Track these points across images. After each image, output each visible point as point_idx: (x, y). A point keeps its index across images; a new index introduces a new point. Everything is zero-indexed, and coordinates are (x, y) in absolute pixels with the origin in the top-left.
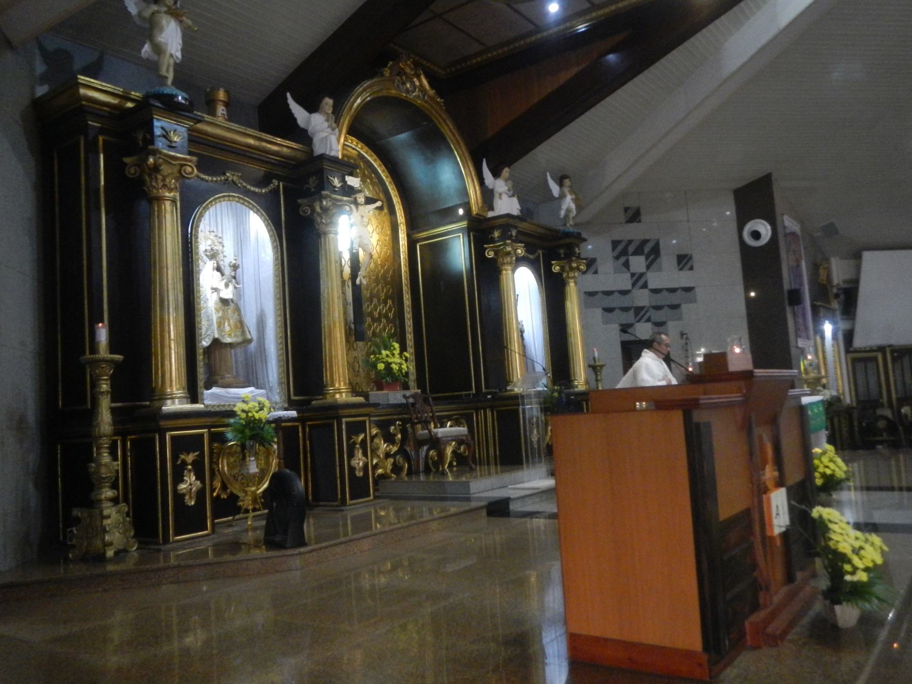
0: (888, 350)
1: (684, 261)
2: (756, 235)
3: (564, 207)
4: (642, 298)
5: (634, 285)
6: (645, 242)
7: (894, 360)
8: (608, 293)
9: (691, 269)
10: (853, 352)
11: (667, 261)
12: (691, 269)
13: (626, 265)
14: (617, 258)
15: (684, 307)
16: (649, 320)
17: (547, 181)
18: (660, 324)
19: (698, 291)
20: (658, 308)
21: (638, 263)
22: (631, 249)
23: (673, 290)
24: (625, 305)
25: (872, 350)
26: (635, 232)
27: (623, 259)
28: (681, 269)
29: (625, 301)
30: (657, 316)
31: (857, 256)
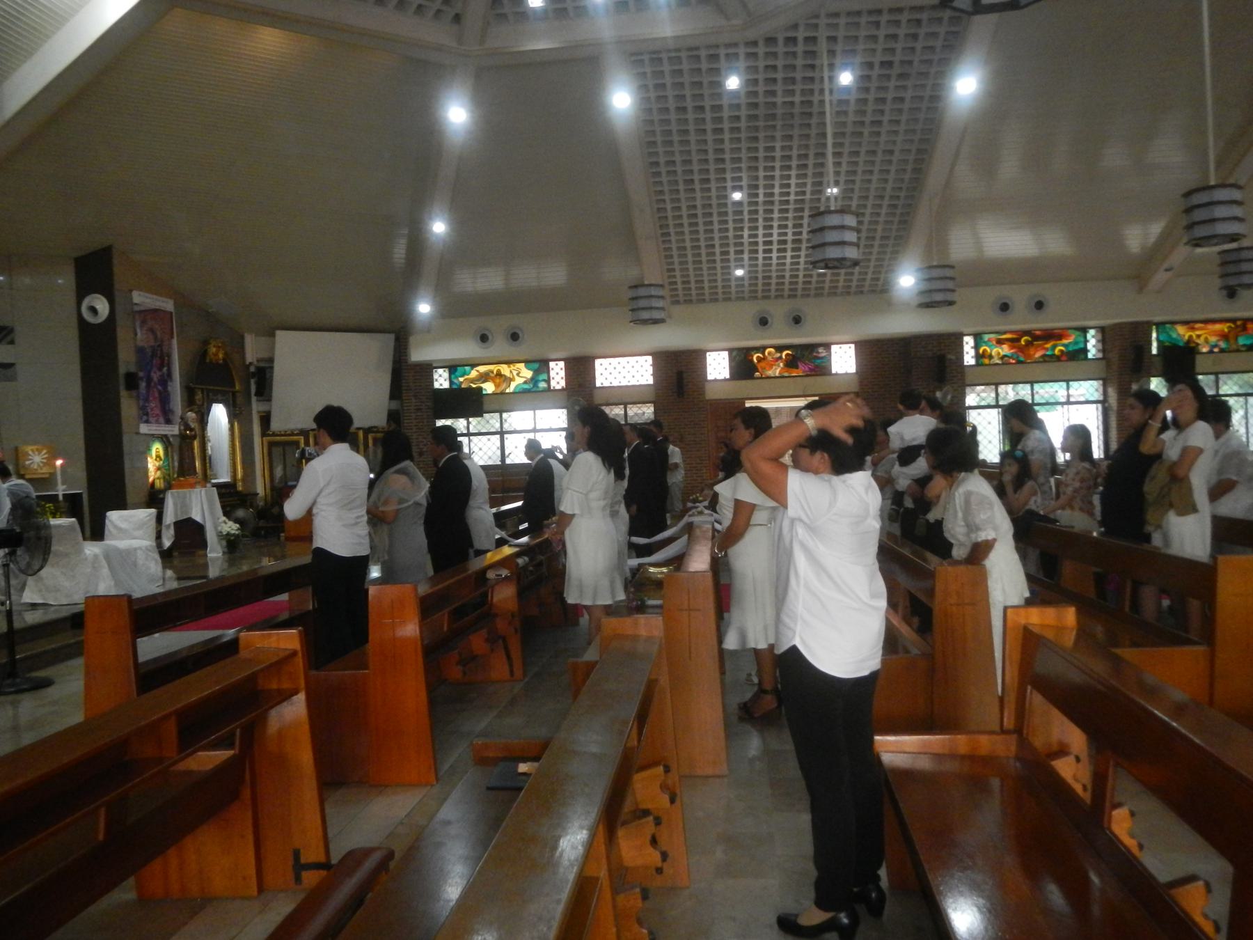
2: (93, 310)
9: (12, 342)
10: (269, 435)
25: (292, 434)
31: (272, 334)
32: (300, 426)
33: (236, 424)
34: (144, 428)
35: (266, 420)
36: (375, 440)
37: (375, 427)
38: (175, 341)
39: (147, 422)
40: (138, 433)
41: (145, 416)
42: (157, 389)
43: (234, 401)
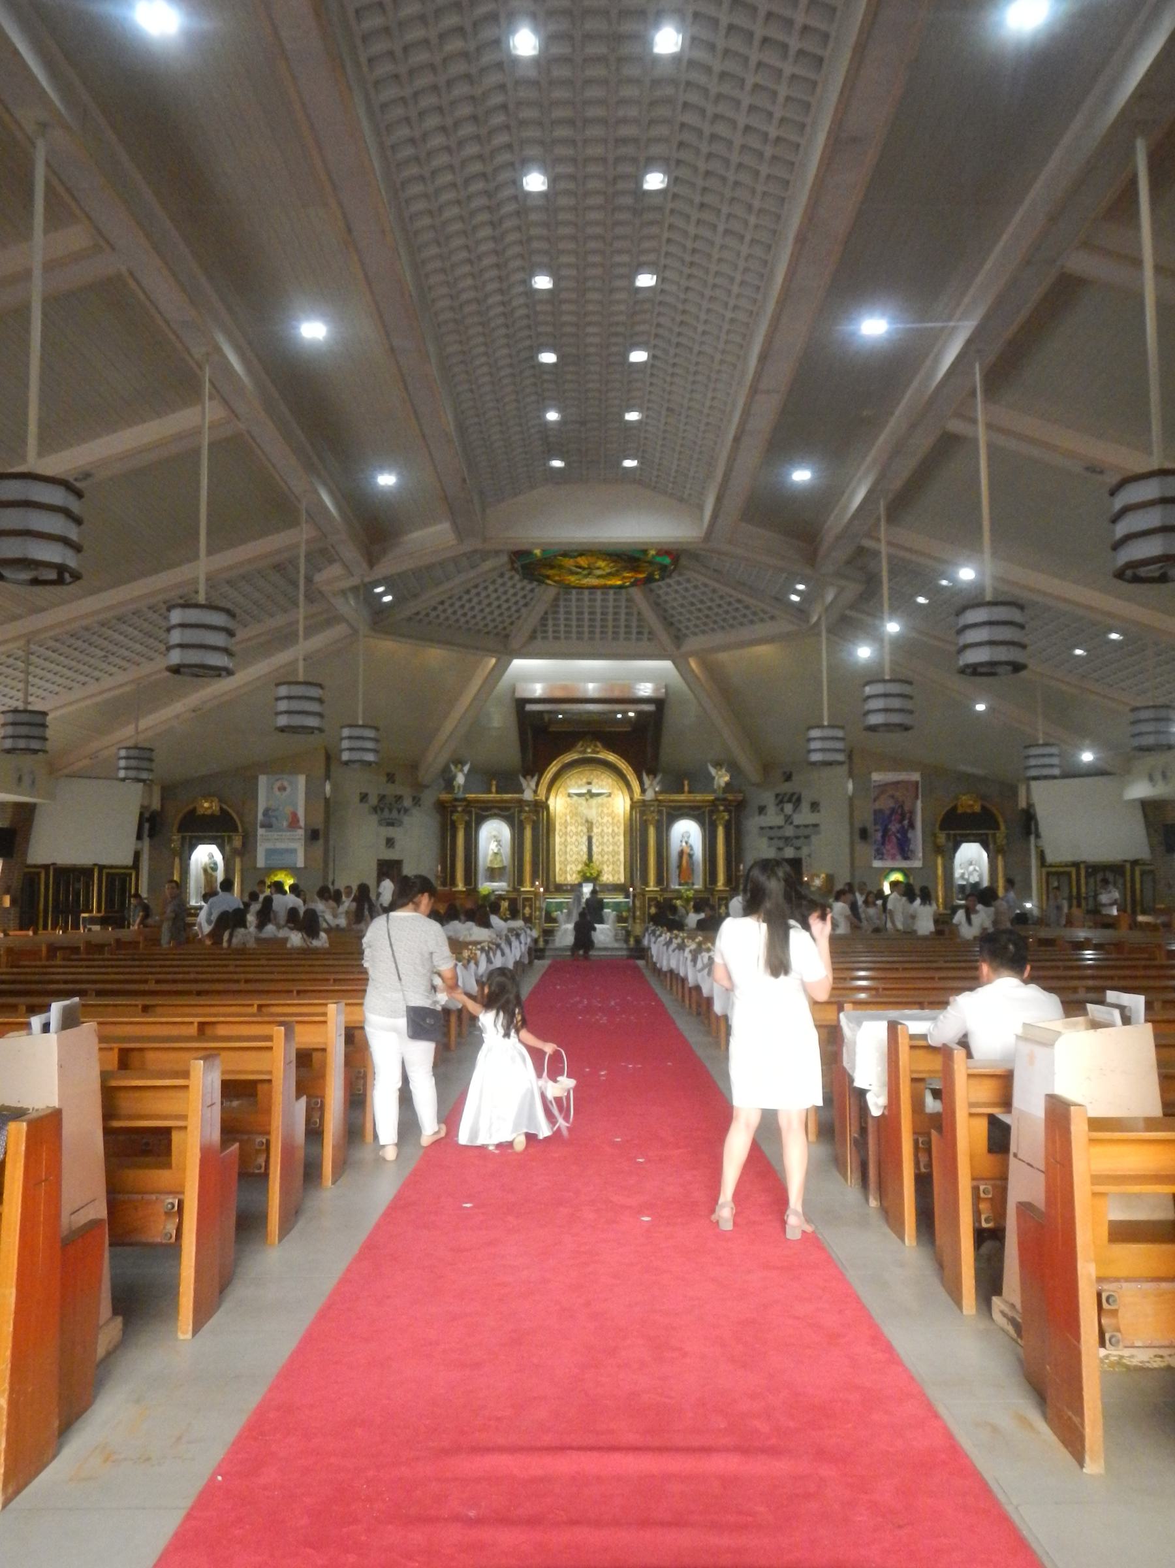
0: (1082, 866)
1: (815, 806)
3: (716, 782)
4: (789, 831)
5: (786, 821)
6: (793, 794)
7: (1088, 875)
8: (771, 828)
9: (818, 811)
11: (805, 806)
12: (818, 811)
13: (782, 810)
14: (777, 805)
15: (814, 839)
16: (792, 846)
17: (707, 769)
18: (798, 848)
19: (822, 827)
20: (797, 838)
21: (788, 808)
22: (786, 799)
23: (806, 826)
24: (780, 835)
25: (1066, 865)
26: (786, 788)
27: (780, 806)
28: (813, 812)
29: (780, 833)
30: (798, 843)
33: (1000, 858)
34: (877, 864)
36: (1143, 873)
37: (1142, 860)
38: (919, 804)
39: (881, 859)
40: (871, 867)
41: (880, 855)
42: (897, 838)
43: (995, 843)
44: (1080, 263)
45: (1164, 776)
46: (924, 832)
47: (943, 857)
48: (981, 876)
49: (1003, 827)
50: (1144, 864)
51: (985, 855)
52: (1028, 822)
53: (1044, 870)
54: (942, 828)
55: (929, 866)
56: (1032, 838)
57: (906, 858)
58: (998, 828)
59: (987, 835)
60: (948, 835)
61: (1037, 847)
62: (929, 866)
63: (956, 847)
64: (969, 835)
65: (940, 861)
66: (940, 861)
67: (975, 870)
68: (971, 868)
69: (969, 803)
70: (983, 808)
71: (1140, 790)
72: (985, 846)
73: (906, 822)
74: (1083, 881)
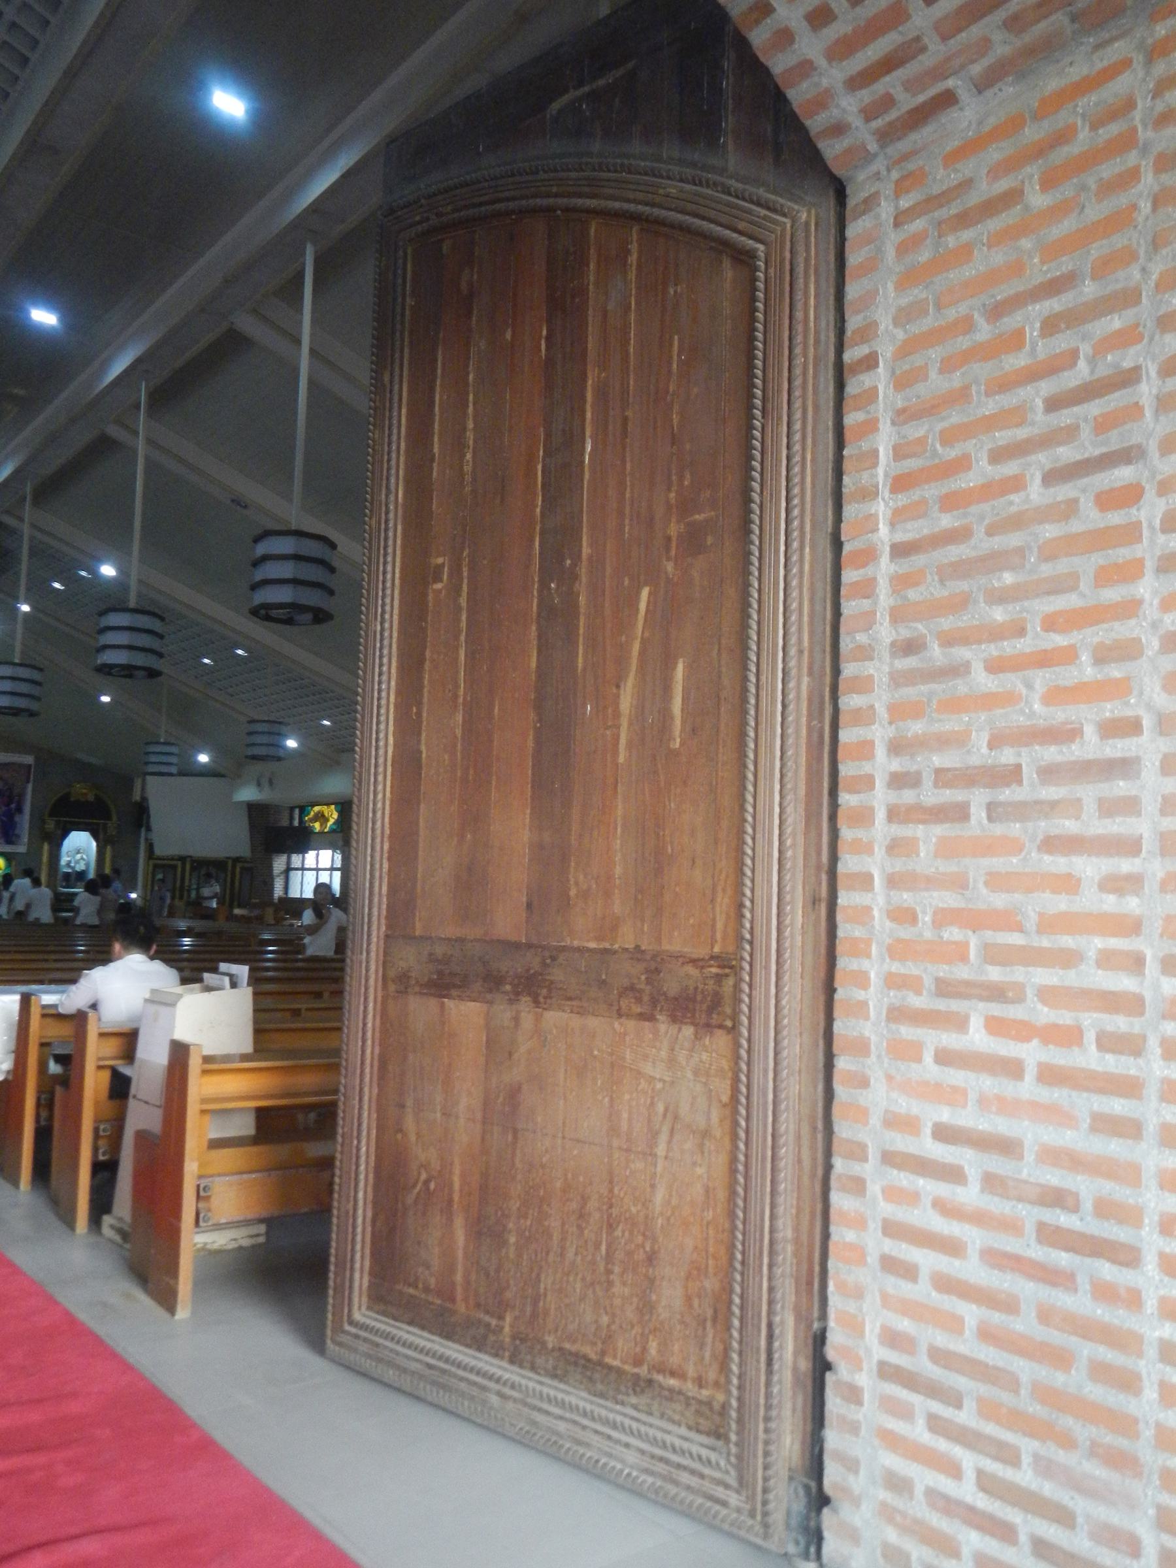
7: (193, 869)
25: (172, 859)
32: (177, 853)
33: (109, 848)
35: (150, 847)
36: (242, 869)
38: (30, 787)
44: (246, 324)
45: (271, 782)
46: (32, 815)
47: (50, 844)
48: (87, 865)
49: (114, 818)
50: (246, 861)
51: (94, 844)
52: (140, 815)
53: (151, 862)
54: (51, 815)
55: (35, 852)
56: (143, 830)
57: (9, 842)
58: (109, 818)
59: (98, 824)
60: (58, 823)
61: (146, 839)
62: (35, 852)
63: (65, 834)
64: (79, 823)
65: (46, 847)
66: (46, 847)
67: (82, 858)
68: (78, 856)
69: (82, 791)
70: (97, 797)
71: (247, 794)
72: (95, 836)
73: (13, 806)
74: (187, 874)
